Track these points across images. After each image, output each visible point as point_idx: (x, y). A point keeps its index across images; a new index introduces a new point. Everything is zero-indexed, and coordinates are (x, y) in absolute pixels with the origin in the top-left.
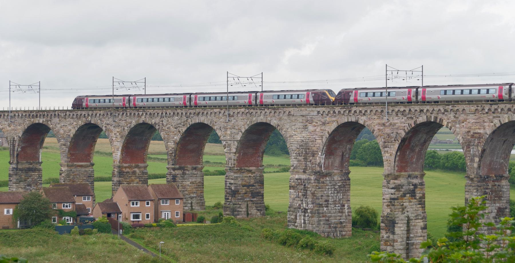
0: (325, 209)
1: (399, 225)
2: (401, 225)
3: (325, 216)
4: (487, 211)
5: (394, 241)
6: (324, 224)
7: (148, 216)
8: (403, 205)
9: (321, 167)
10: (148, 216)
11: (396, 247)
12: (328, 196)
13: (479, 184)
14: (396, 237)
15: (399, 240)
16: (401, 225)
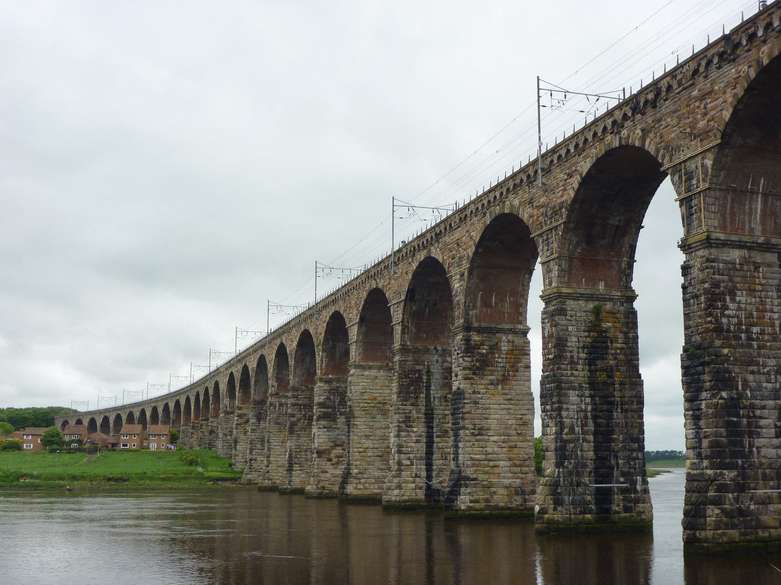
0: (229, 437)
1: (241, 444)
2: (243, 444)
3: (229, 443)
4: (261, 427)
5: (236, 455)
6: (227, 448)
7: (134, 445)
8: (245, 429)
9: (226, 407)
10: (134, 445)
11: (237, 460)
12: (232, 428)
13: (254, 406)
14: (237, 453)
15: (241, 455)
16: (243, 444)
